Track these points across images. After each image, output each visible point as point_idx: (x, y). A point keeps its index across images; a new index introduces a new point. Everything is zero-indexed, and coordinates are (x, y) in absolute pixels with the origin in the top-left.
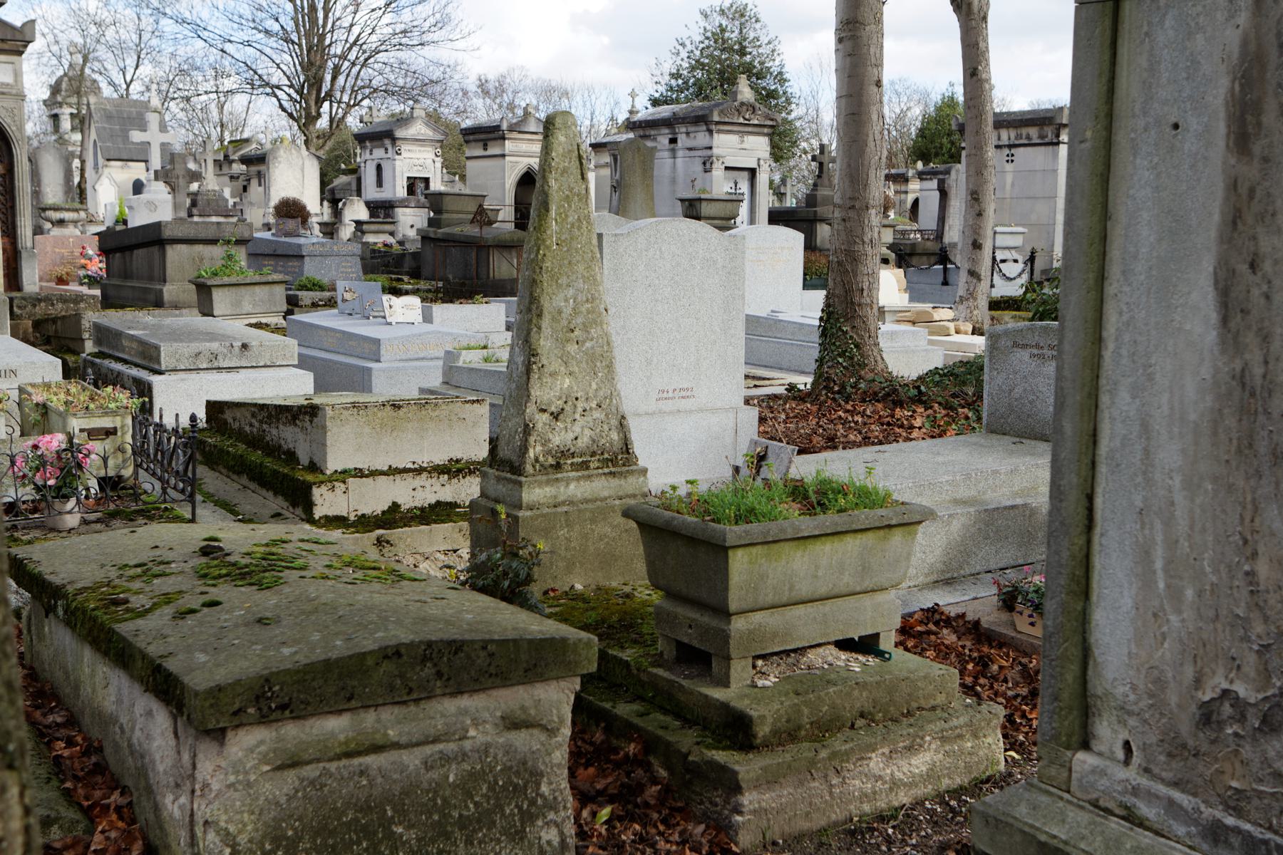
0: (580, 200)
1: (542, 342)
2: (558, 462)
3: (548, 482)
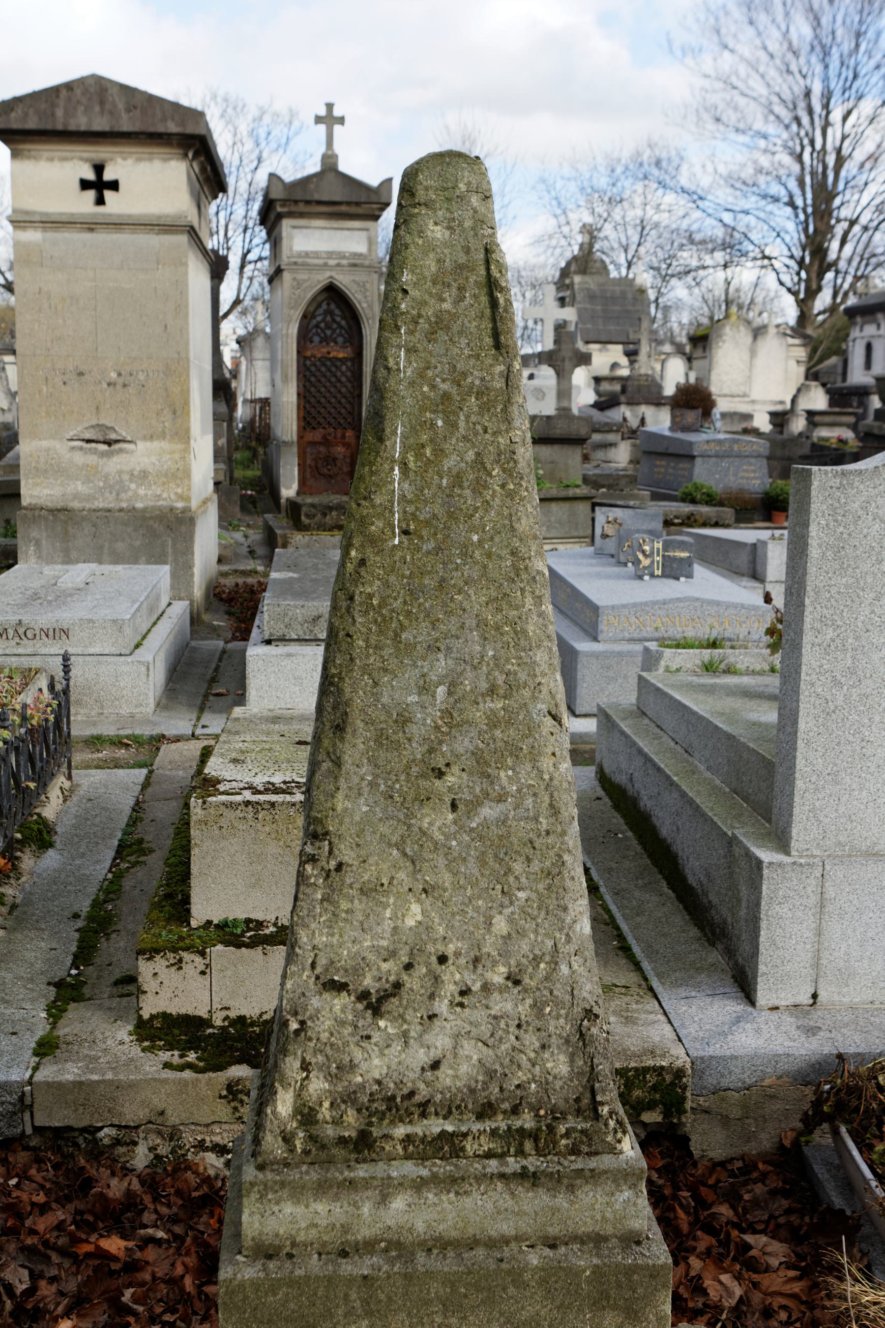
0: (485, 408)
1: (341, 803)
2: (362, 1135)
3: (322, 1189)
